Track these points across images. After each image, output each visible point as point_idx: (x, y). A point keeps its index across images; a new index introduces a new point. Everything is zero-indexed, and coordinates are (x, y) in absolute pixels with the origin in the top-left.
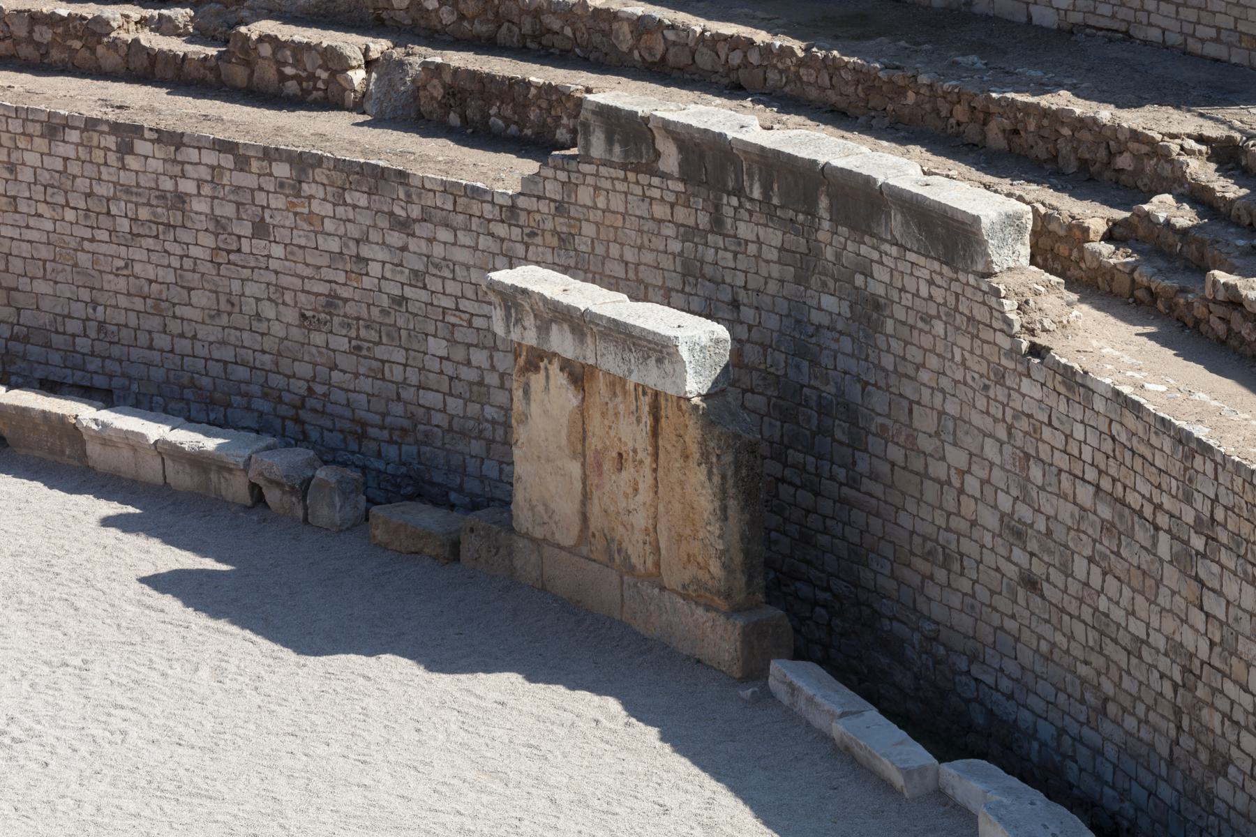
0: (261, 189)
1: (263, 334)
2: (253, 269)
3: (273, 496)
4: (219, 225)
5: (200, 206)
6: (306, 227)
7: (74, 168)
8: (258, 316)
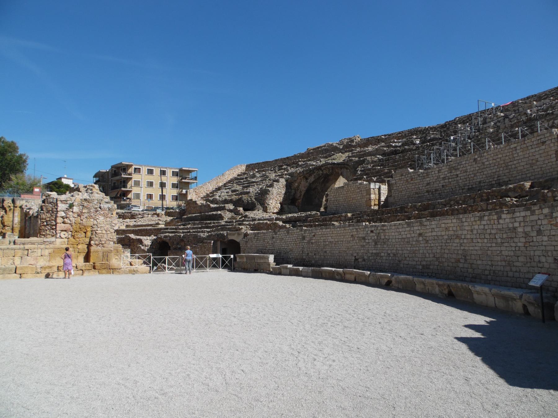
0: (539, 219)
1: (541, 268)
2: (537, 246)
3: (531, 309)
4: (526, 234)
5: (520, 230)
6: (555, 228)
7: (486, 227)
8: (539, 262)
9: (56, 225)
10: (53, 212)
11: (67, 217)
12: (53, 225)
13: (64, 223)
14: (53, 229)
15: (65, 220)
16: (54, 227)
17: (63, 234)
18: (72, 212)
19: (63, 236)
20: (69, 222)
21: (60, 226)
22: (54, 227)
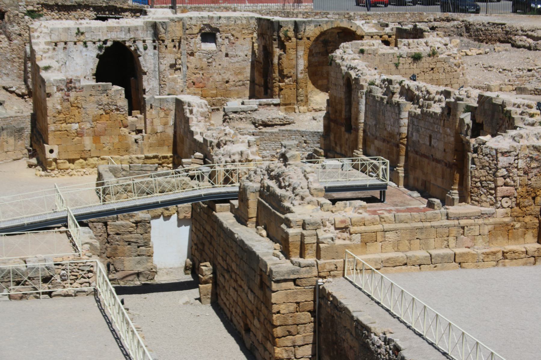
9: (495, 189)
10: (490, 169)
11: (509, 177)
12: (491, 189)
13: (506, 185)
14: (492, 194)
15: (508, 180)
16: (493, 192)
17: (506, 203)
18: (516, 167)
19: (505, 205)
20: (512, 183)
21: (502, 190)
22: (493, 192)
